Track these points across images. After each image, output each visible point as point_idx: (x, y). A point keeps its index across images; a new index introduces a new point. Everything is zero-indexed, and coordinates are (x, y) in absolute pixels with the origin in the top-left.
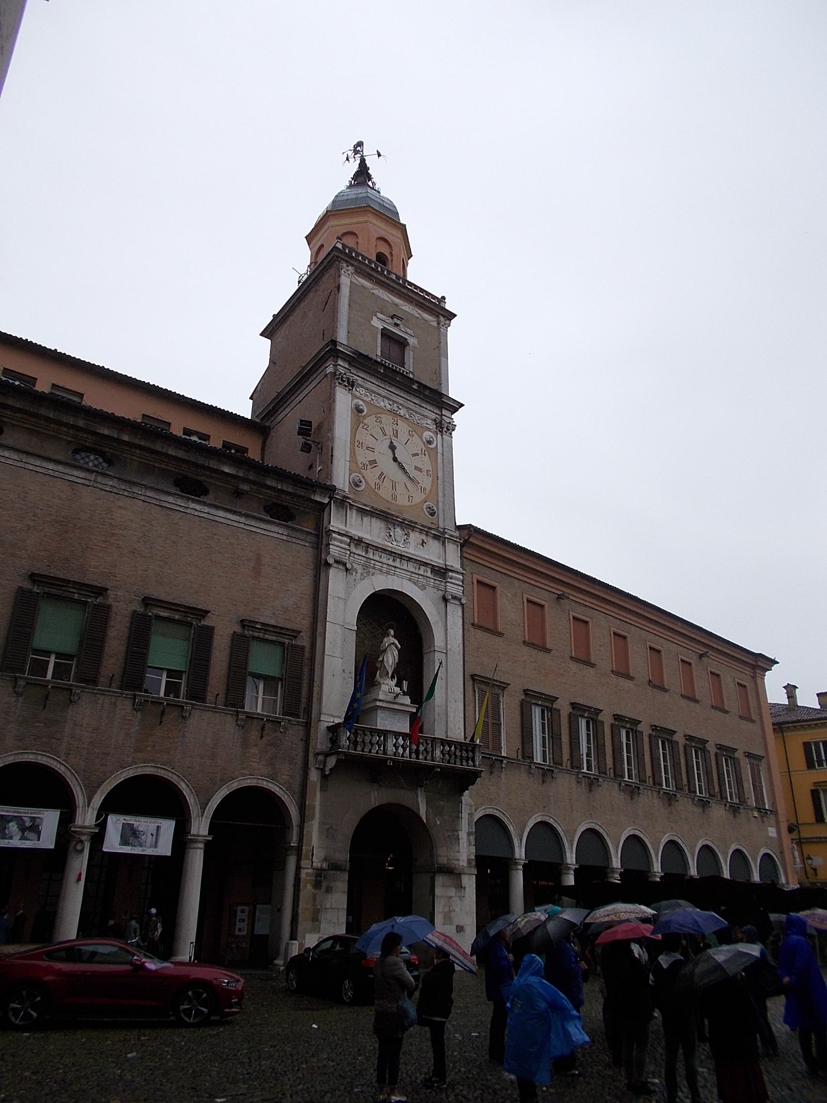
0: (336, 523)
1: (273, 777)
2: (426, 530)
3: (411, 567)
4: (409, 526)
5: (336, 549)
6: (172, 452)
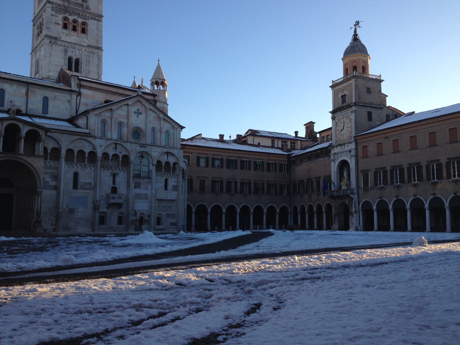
0: (332, 152)
1: (329, 201)
2: (348, 143)
3: (345, 153)
4: (344, 144)
5: (331, 158)
6: (314, 153)
